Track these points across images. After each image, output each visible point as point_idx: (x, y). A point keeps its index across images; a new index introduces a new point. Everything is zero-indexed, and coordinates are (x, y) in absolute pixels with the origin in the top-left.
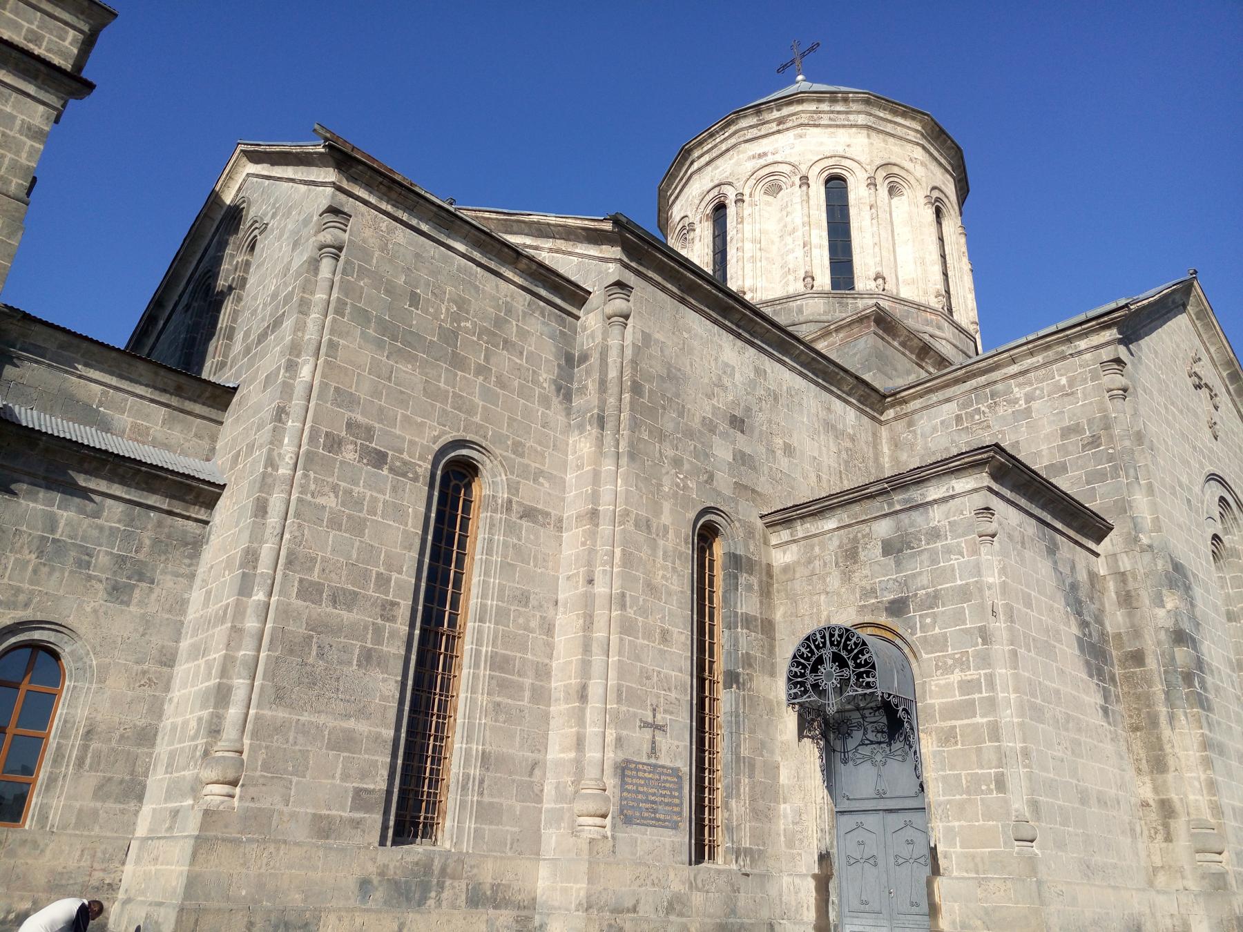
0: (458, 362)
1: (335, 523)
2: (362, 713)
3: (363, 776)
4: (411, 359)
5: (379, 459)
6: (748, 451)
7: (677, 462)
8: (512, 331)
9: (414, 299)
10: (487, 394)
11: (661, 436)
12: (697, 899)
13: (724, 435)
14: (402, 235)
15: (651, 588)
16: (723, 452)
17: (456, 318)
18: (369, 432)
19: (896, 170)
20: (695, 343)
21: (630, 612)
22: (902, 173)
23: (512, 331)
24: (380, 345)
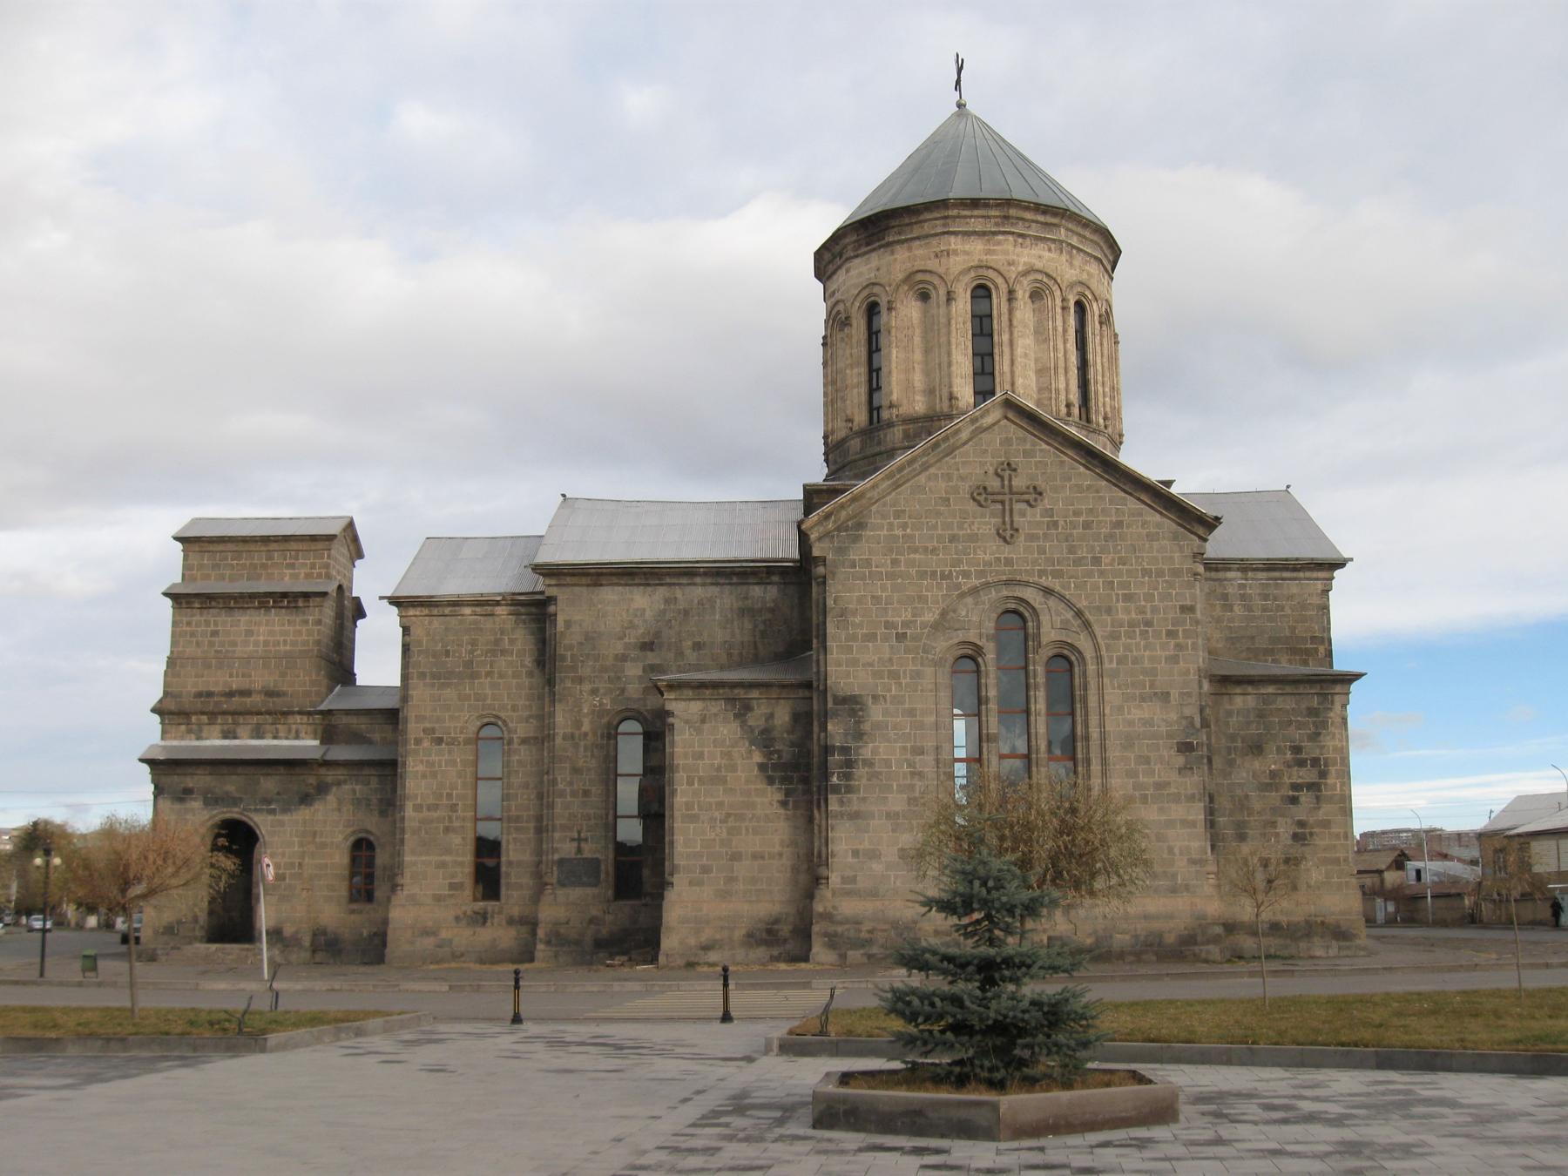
0: (474, 676)
1: (424, 776)
2: (448, 851)
3: (453, 877)
4: (448, 685)
5: (439, 741)
6: (657, 661)
7: (594, 692)
8: (506, 644)
9: (447, 653)
10: (494, 686)
11: (580, 680)
12: (609, 918)
13: (633, 660)
14: (436, 622)
15: (576, 771)
16: (633, 670)
17: (471, 652)
18: (433, 730)
19: (919, 277)
20: (609, 608)
21: (561, 786)
22: (927, 277)
23: (506, 644)
24: (433, 685)
